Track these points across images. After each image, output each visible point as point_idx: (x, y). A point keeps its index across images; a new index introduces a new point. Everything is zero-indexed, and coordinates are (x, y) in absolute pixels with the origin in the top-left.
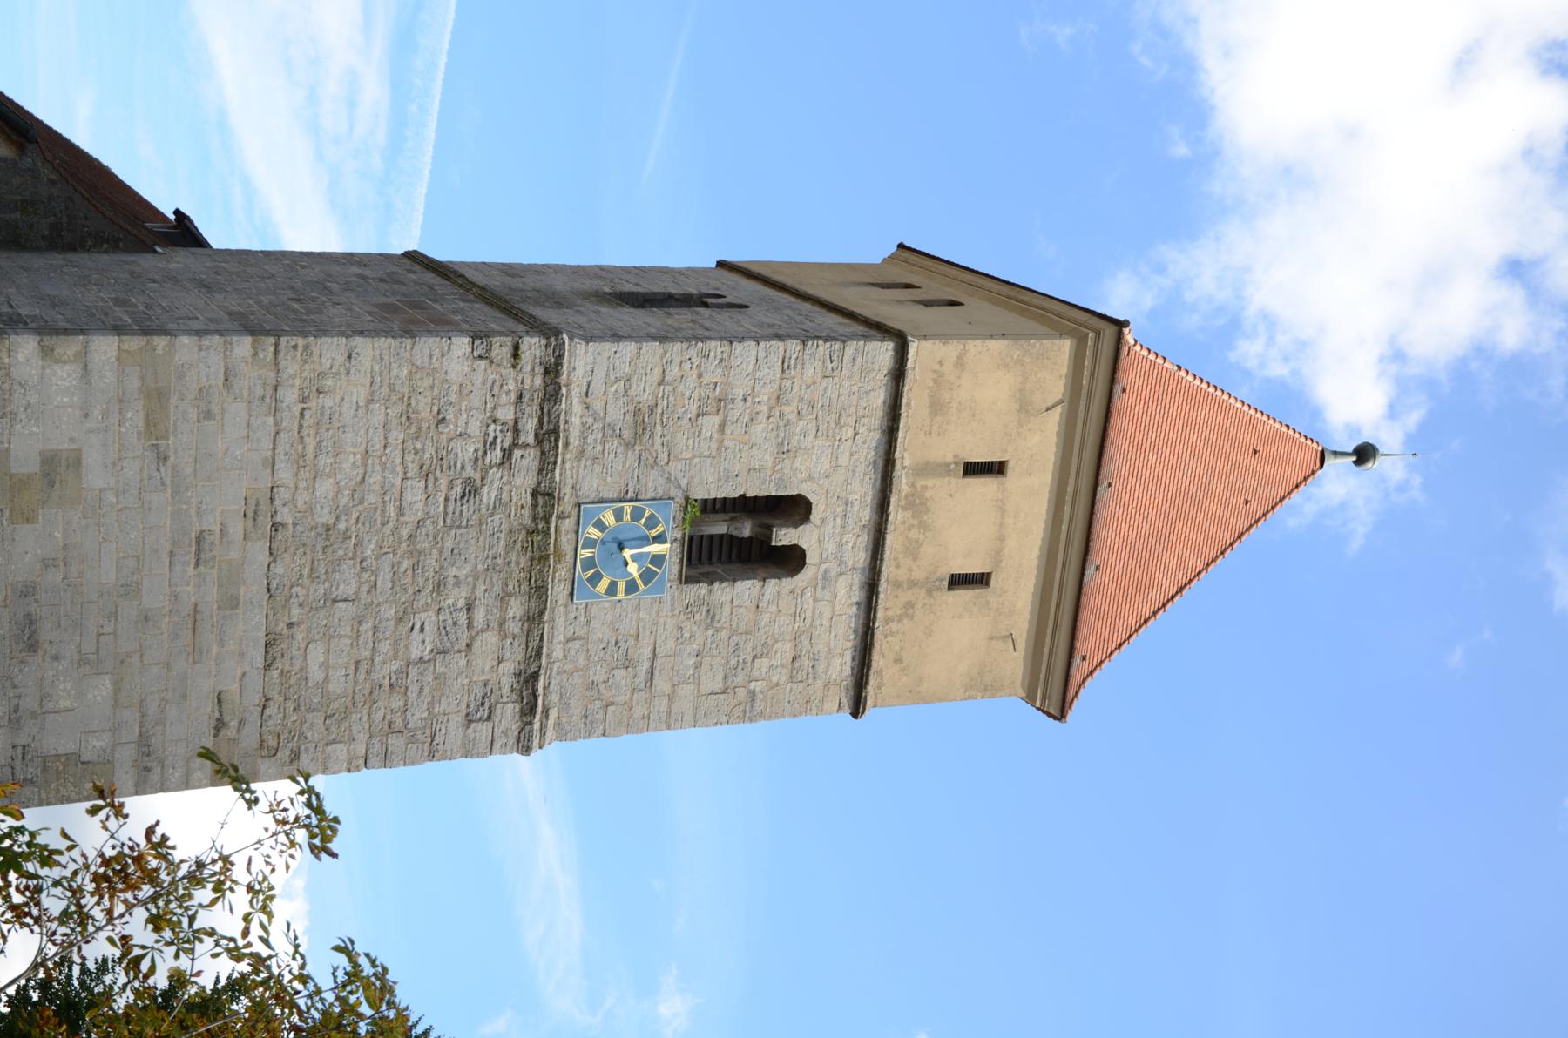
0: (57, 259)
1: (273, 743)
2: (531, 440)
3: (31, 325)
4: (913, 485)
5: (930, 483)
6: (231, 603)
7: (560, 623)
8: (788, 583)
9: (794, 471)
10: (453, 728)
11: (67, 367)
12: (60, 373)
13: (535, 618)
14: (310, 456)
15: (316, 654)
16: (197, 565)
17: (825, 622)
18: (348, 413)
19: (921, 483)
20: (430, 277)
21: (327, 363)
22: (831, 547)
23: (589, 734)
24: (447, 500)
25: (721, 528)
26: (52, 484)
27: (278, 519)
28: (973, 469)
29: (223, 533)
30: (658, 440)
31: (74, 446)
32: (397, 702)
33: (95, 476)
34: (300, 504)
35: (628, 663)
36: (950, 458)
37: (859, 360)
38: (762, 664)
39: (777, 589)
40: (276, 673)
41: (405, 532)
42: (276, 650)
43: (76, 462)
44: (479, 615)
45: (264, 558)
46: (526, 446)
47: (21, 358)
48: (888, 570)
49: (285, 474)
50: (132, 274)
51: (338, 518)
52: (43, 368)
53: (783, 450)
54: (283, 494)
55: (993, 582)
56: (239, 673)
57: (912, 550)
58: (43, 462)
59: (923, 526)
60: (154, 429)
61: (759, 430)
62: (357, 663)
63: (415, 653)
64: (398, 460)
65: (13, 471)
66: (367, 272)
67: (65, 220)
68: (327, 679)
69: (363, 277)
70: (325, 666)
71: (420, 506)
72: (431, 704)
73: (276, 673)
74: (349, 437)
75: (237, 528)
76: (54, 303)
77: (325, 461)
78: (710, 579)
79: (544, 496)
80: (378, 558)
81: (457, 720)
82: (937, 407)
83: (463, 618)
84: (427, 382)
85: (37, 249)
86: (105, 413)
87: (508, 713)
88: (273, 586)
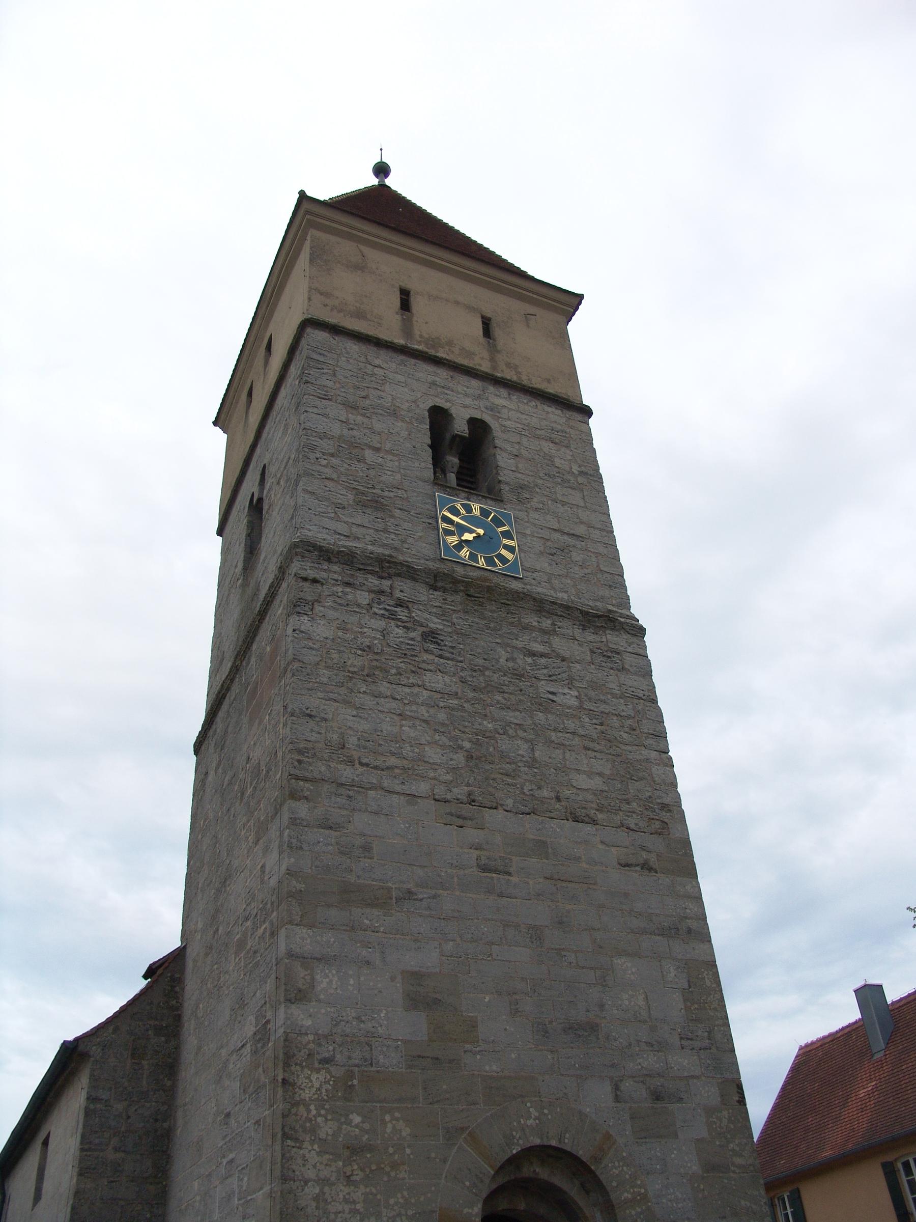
0: (189, 1026)
3: (269, 1015)
8: (498, 434)
11: (318, 977)
12: (324, 985)
13: (542, 606)
15: (581, 781)
16: (510, 874)
18: (364, 726)
20: (221, 714)
21: (314, 737)
22: (468, 401)
24: (441, 657)
26: (437, 1002)
27: (465, 799)
30: (386, 494)
32: (615, 722)
34: (449, 777)
35: (564, 549)
36: (398, 317)
37: (321, 351)
38: (558, 462)
40: (600, 816)
42: (581, 813)
43: (416, 977)
44: (538, 647)
45: (500, 814)
46: (391, 587)
49: (423, 787)
50: (207, 954)
51: (461, 748)
52: (319, 1001)
53: (394, 413)
54: (440, 791)
55: (489, 315)
56: (600, 846)
57: (470, 354)
60: (379, 900)
61: (378, 426)
63: (574, 702)
64: (407, 690)
65: (426, 1038)
67: (152, 1022)
68: (600, 774)
70: (590, 774)
71: (447, 679)
72: (614, 696)
73: (600, 816)
75: (472, 834)
76: (242, 1002)
81: (623, 678)
82: (360, 315)
83: (543, 661)
84: (335, 656)
85: (178, 1047)
88: (527, 810)
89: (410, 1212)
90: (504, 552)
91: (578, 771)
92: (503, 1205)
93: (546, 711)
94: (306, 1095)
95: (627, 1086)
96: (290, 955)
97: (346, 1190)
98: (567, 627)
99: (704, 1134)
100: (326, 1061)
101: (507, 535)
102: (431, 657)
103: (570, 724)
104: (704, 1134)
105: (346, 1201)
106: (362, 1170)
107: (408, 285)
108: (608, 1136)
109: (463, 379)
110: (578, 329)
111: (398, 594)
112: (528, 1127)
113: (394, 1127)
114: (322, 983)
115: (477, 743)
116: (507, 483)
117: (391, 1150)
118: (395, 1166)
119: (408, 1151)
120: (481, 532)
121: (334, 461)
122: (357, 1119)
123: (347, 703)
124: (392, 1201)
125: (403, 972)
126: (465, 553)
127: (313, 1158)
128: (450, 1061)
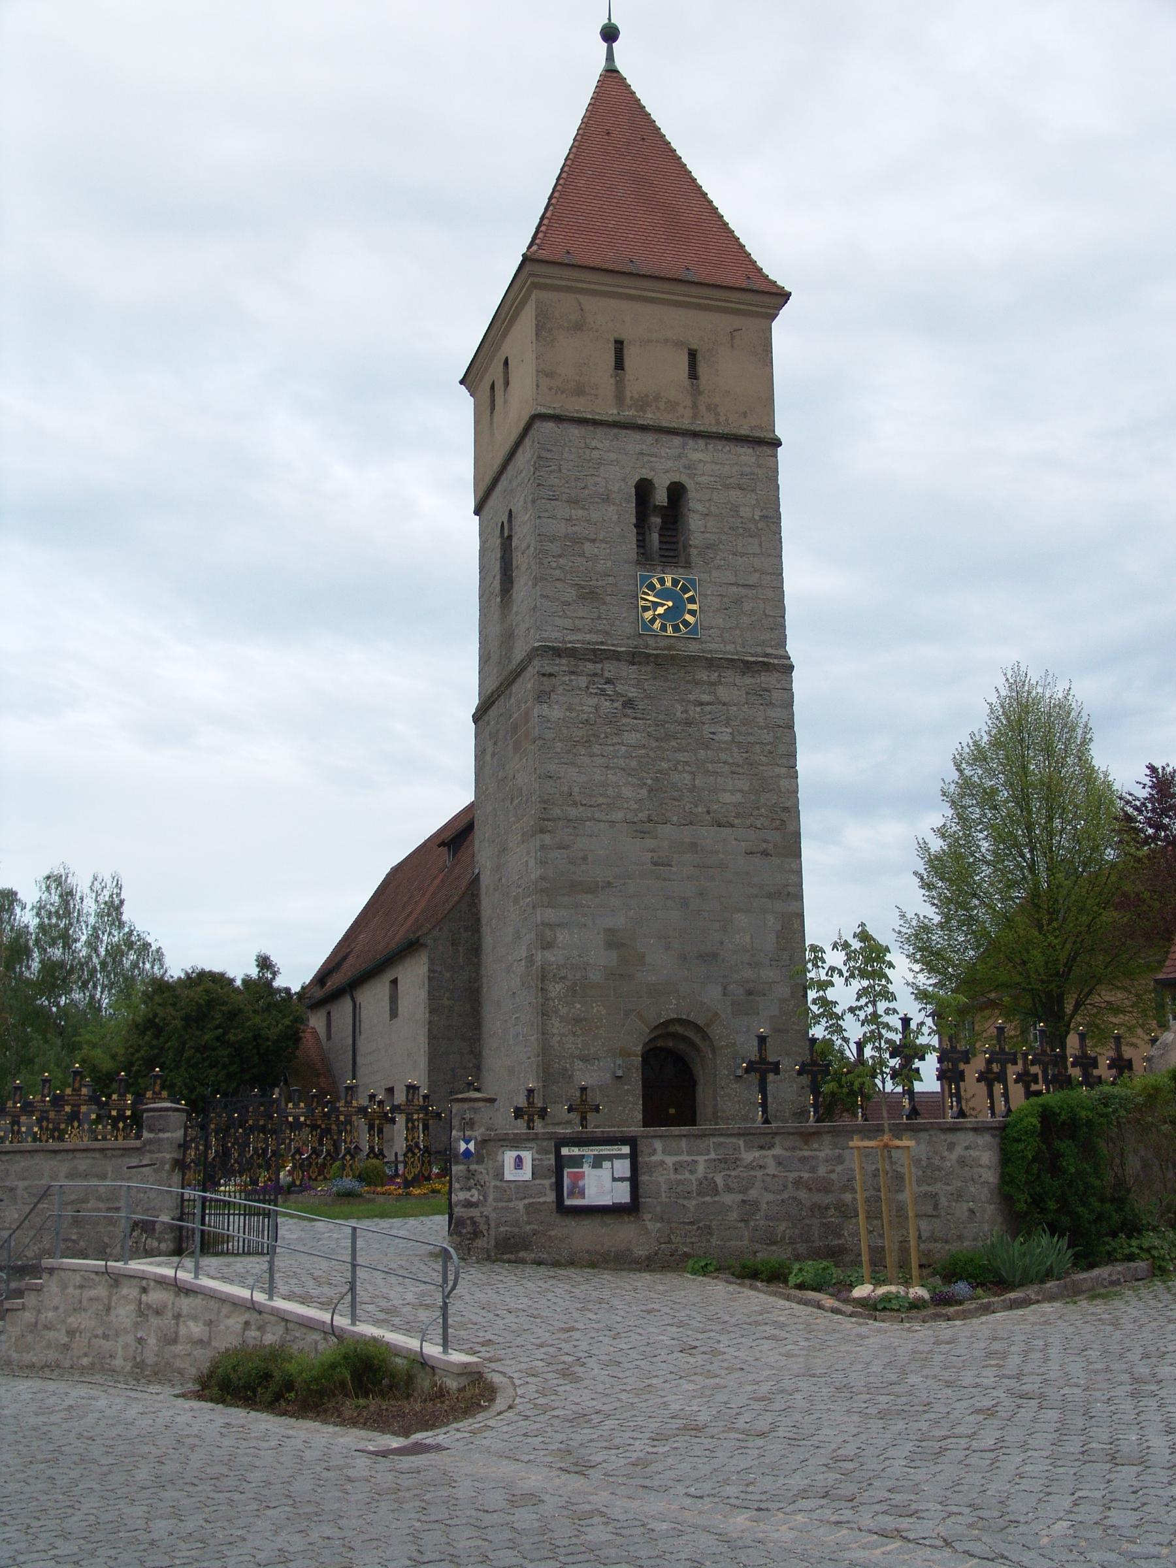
0: (486, 930)
1: (778, 822)
2: (599, 666)
4: (630, 407)
5: (628, 394)
6: (693, 847)
7: (713, 646)
8: (692, 494)
9: (620, 490)
10: (776, 714)
13: (711, 663)
14: (609, 800)
15: (727, 798)
17: (718, 467)
19: (628, 401)
21: (554, 790)
22: (670, 464)
23: (784, 627)
24: (635, 718)
25: (655, 537)
26: (623, 945)
28: (619, 364)
29: (653, 851)
30: (600, 583)
33: (619, 921)
34: (636, 806)
35: (738, 601)
36: (612, 381)
37: (549, 447)
38: (745, 511)
39: (696, 502)
40: (736, 821)
41: (655, 744)
42: (723, 820)
43: (611, 932)
44: (706, 698)
46: (602, 669)
47: (553, 959)
48: (686, 423)
51: (645, 784)
53: (607, 499)
55: (695, 347)
57: (672, 406)
59: (657, 398)
62: (733, 773)
63: (728, 738)
64: (611, 748)
66: (490, 750)
68: (741, 791)
69: (493, 755)
70: (733, 792)
71: (638, 735)
72: (760, 728)
74: (597, 777)
75: (650, 843)
77: (610, 791)
78: (686, 546)
79: (634, 658)
80: (669, 761)
82: (580, 391)
83: (708, 708)
85: (479, 939)
86: (584, 915)
87: (765, 679)
90: (688, 617)
91: (724, 790)
92: (660, 1044)
93: (707, 748)
94: (553, 995)
95: (732, 987)
96: (543, 924)
98: (730, 676)
99: (777, 1013)
100: (562, 978)
101: (692, 600)
102: (628, 720)
103: (723, 756)
104: (777, 1013)
107: (623, 336)
108: (716, 1014)
109: (665, 438)
110: (785, 332)
111: (607, 674)
112: (670, 1009)
114: (560, 938)
115: (656, 780)
116: (696, 547)
118: (597, 1028)
120: (670, 604)
121: (562, 561)
122: (579, 1006)
123: (572, 764)
125: (605, 930)
126: (657, 625)
127: (557, 1024)
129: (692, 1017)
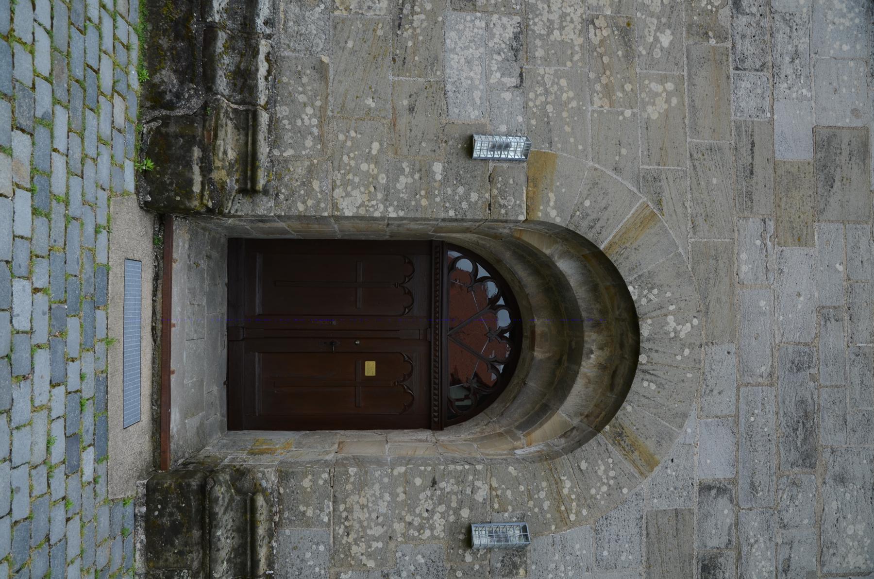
26: (830, 182)
31: (858, 123)
58: (818, 146)
89: (550, 108)
95: (723, 510)
97: (577, 19)
105: (563, 16)
106: (602, 42)
108: (651, 463)
113: (657, 95)
117: (628, 87)
118: (608, 91)
119: (628, 113)
122: (666, 39)
124: (563, 82)
125: (866, 129)
128: (749, 194)
129: (641, 385)
